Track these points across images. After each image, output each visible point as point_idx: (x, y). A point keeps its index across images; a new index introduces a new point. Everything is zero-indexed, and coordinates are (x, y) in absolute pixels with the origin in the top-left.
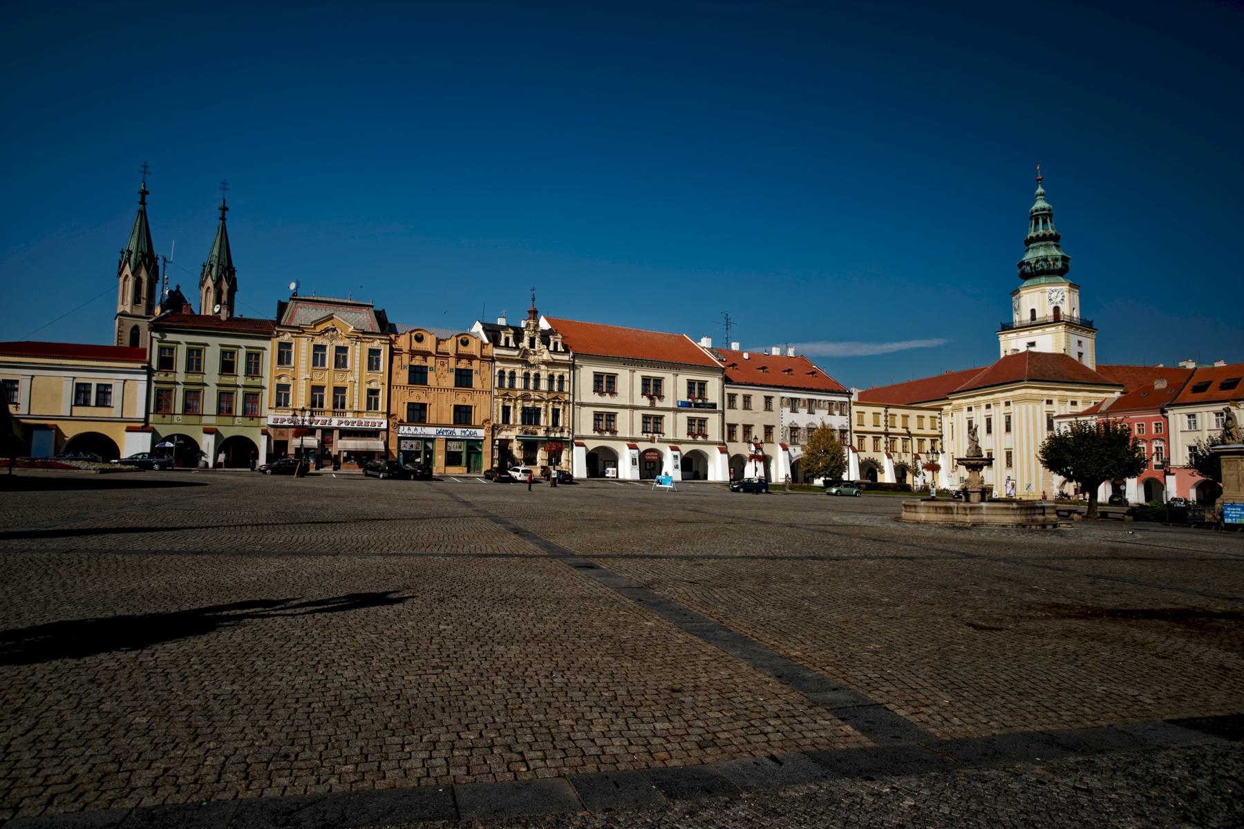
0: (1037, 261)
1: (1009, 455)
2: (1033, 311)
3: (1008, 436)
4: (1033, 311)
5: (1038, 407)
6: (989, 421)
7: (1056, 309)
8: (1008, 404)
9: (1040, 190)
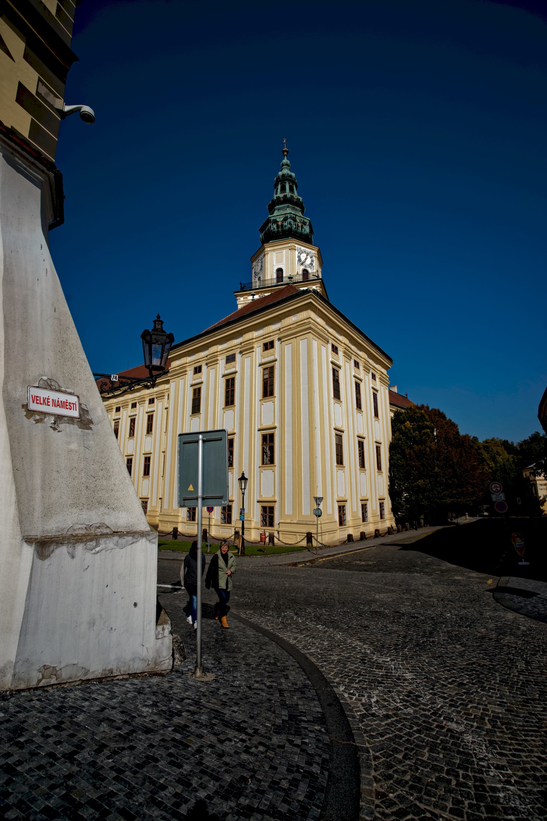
0: (285, 219)
1: (268, 440)
2: (280, 271)
3: (268, 404)
4: (280, 271)
5: (323, 349)
6: (230, 384)
7: (305, 272)
8: (268, 346)
9: (285, 161)
